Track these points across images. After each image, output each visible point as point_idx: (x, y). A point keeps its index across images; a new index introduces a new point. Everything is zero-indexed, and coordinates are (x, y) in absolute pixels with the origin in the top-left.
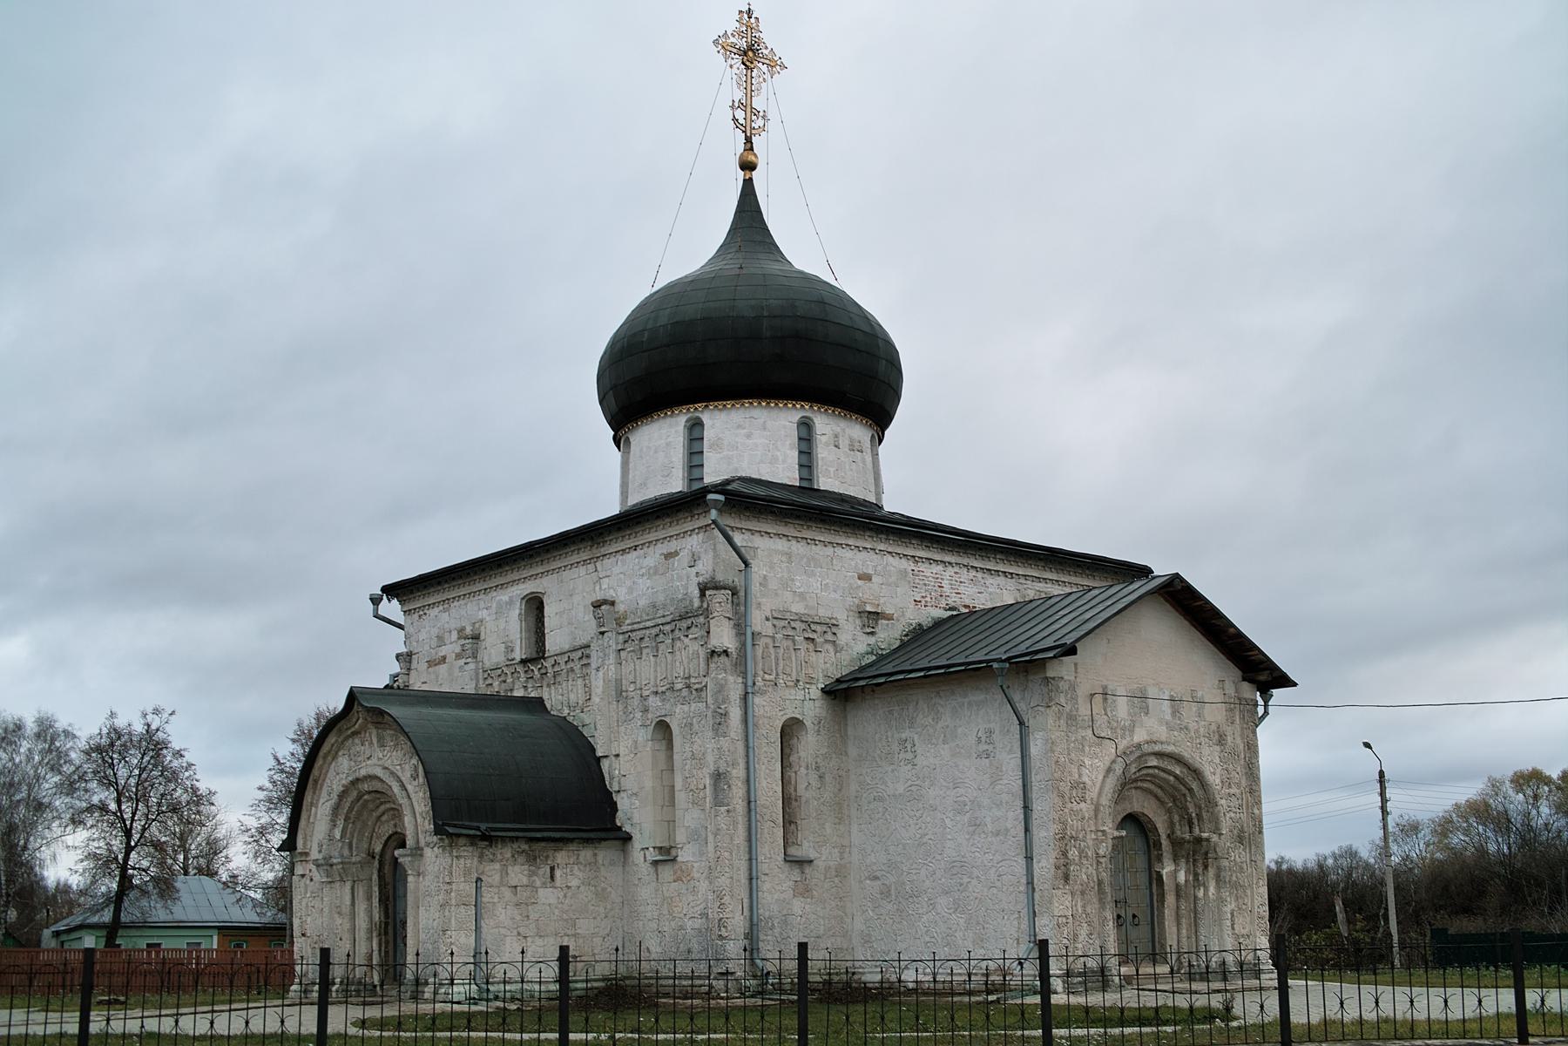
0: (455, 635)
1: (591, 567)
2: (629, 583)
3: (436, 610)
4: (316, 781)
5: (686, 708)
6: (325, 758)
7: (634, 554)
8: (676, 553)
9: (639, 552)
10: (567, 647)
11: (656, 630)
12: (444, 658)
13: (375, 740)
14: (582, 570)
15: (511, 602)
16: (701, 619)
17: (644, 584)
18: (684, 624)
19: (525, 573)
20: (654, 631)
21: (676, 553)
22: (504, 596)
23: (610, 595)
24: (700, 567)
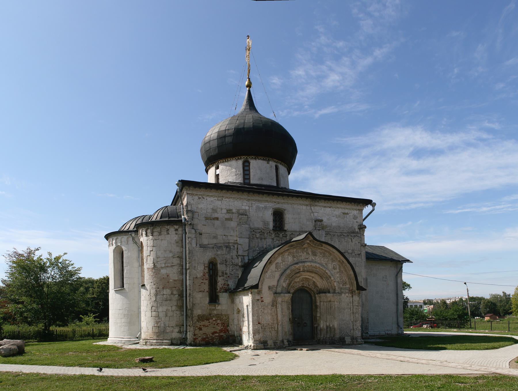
0: (224, 211)
1: (308, 207)
2: (328, 217)
3: (212, 199)
4: (270, 263)
5: (354, 259)
6: (279, 255)
7: (329, 209)
8: (348, 214)
9: (331, 209)
10: (298, 230)
11: (339, 234)
12: (217, 219)
13: (310, 253)
14: (304, 207)
15: (266, 208)
16: (359, 235)
17: (334, 219)
18: (353, 235)
19: (274, 200)
20: (339, 234)
21: (348, 214)
22: (262, 205)
23: (320, 218)
24: (358, 220)
